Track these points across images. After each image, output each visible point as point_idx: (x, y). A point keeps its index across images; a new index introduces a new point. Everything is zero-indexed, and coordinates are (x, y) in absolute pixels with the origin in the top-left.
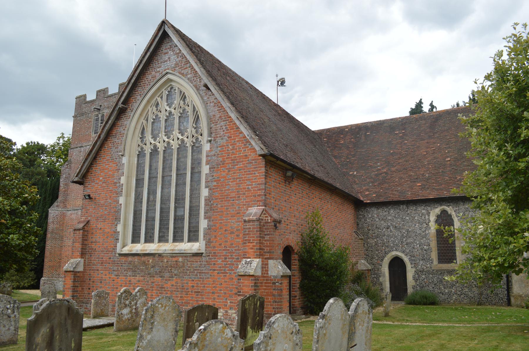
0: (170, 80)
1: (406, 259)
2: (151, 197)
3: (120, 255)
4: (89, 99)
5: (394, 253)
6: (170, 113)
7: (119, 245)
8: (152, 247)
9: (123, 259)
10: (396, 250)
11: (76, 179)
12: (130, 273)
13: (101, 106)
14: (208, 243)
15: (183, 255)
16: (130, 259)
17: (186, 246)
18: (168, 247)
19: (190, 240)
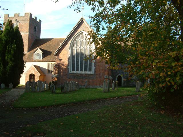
0: (82, 33)
1: (122, 76)
2: (77, 61)
3: (70, 74)
4: (9, 16)
5: (119, 75)
6: (82, 40)
7: (69, 72)
8: (79, 72)
9: (71, 75)
10: (120, 74)
11: (55, 54)
12: (73, 78)
13: (16, 20)
14: (95, 72)
15: (89, 74)
16: (73, 75)
17: (88, 72)
18: (84, 72)
19: (89, 71)
